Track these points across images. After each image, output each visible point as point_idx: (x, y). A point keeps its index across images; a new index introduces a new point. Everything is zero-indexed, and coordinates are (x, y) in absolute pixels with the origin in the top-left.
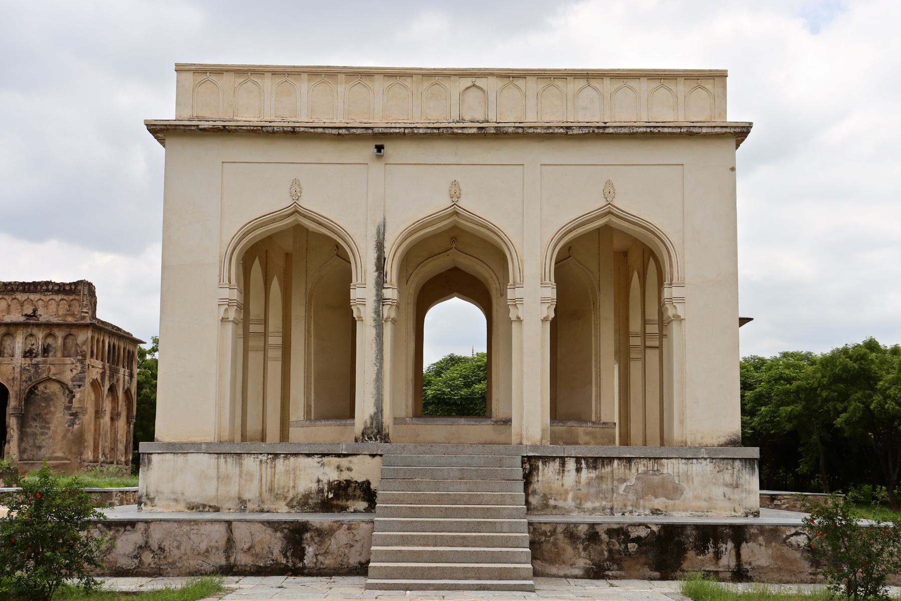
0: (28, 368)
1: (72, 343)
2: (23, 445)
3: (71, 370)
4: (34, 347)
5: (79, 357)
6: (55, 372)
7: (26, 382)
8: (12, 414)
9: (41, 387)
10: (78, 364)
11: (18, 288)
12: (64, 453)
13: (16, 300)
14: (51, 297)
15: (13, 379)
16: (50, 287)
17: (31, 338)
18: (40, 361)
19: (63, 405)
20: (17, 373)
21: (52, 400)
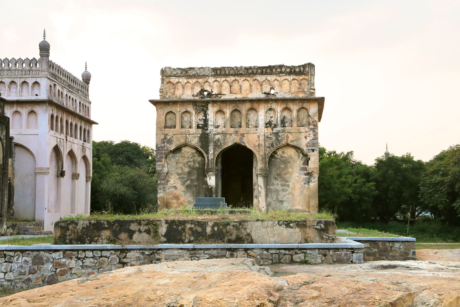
0: (270, 136)
1: (304, 115)
2: (269, 199)
3: (306, 137)
4: (272, 119)
5: (311, 127)
6: (292, 139)
7: (269, 148)
8: (259, 174)
9: (280, 152)
10: (311, 132)
11: (257, 72)
12: (303, 206)
13: (256, 81)
14: (285, 77)
15: (259, 145)
16: (283, 69)
17: (270, 112)
18: (280, 131)
19: (299, 166)
20: (262, 140)
21: (289, 162)
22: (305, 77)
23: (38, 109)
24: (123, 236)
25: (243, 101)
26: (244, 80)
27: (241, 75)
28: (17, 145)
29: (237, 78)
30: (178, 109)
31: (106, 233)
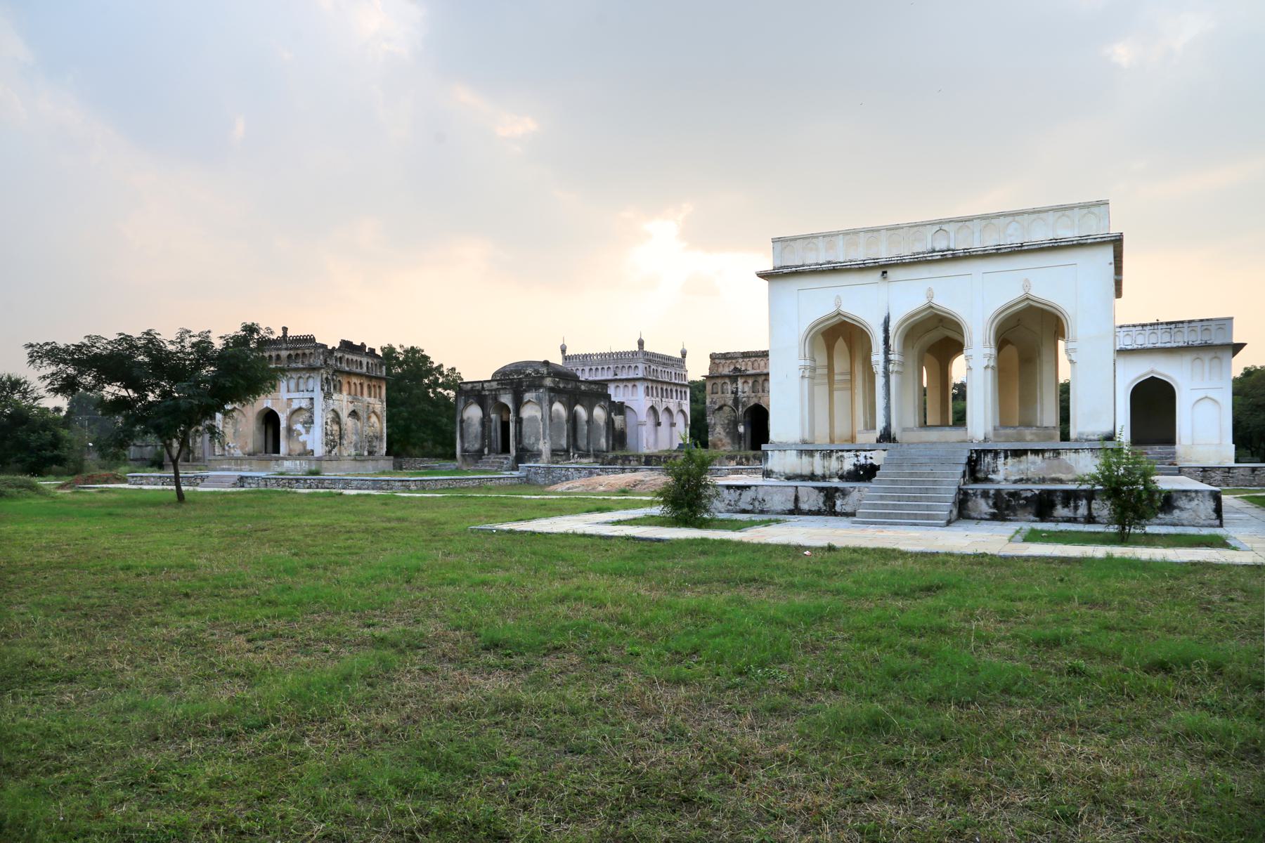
23: (638, 384)
24: (627, 462)
27: (759, 356)
28: (627, 407)
30: (720, 381)
31: (620, 461)
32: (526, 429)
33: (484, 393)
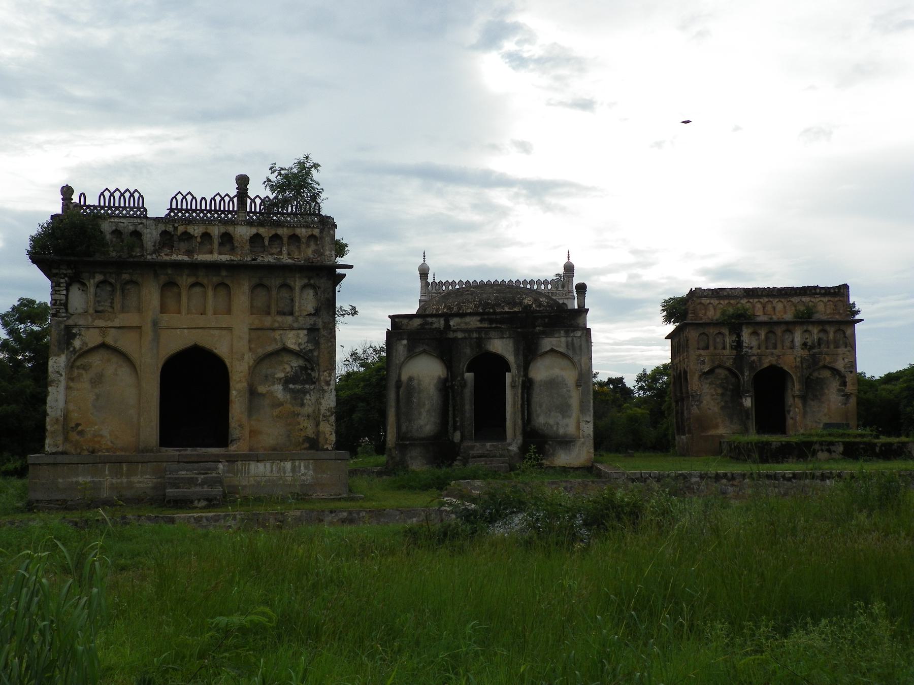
3: (843, 359)
4: (808, 340)
8: (797, 396)
11: (790, 293)
13: (790, 302)
14: (820, 299)
15: (795, 367)
18: (816, 352)
20: (798, 362)
22: (841, 299)
25: (779, 323)
26: (777, 302)
27: (774, 296)
29: (771, 300)
32: (539, 397)
33: (451, 335)
